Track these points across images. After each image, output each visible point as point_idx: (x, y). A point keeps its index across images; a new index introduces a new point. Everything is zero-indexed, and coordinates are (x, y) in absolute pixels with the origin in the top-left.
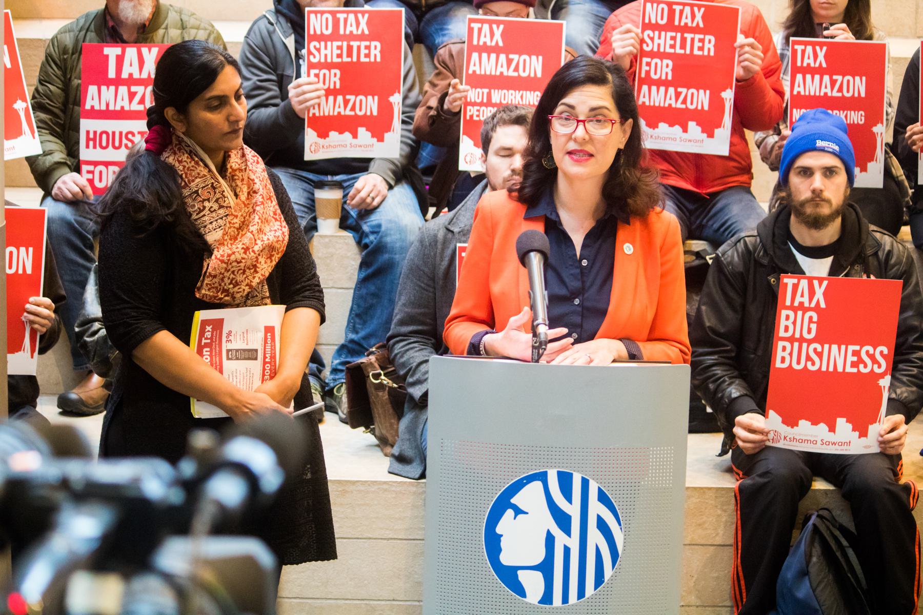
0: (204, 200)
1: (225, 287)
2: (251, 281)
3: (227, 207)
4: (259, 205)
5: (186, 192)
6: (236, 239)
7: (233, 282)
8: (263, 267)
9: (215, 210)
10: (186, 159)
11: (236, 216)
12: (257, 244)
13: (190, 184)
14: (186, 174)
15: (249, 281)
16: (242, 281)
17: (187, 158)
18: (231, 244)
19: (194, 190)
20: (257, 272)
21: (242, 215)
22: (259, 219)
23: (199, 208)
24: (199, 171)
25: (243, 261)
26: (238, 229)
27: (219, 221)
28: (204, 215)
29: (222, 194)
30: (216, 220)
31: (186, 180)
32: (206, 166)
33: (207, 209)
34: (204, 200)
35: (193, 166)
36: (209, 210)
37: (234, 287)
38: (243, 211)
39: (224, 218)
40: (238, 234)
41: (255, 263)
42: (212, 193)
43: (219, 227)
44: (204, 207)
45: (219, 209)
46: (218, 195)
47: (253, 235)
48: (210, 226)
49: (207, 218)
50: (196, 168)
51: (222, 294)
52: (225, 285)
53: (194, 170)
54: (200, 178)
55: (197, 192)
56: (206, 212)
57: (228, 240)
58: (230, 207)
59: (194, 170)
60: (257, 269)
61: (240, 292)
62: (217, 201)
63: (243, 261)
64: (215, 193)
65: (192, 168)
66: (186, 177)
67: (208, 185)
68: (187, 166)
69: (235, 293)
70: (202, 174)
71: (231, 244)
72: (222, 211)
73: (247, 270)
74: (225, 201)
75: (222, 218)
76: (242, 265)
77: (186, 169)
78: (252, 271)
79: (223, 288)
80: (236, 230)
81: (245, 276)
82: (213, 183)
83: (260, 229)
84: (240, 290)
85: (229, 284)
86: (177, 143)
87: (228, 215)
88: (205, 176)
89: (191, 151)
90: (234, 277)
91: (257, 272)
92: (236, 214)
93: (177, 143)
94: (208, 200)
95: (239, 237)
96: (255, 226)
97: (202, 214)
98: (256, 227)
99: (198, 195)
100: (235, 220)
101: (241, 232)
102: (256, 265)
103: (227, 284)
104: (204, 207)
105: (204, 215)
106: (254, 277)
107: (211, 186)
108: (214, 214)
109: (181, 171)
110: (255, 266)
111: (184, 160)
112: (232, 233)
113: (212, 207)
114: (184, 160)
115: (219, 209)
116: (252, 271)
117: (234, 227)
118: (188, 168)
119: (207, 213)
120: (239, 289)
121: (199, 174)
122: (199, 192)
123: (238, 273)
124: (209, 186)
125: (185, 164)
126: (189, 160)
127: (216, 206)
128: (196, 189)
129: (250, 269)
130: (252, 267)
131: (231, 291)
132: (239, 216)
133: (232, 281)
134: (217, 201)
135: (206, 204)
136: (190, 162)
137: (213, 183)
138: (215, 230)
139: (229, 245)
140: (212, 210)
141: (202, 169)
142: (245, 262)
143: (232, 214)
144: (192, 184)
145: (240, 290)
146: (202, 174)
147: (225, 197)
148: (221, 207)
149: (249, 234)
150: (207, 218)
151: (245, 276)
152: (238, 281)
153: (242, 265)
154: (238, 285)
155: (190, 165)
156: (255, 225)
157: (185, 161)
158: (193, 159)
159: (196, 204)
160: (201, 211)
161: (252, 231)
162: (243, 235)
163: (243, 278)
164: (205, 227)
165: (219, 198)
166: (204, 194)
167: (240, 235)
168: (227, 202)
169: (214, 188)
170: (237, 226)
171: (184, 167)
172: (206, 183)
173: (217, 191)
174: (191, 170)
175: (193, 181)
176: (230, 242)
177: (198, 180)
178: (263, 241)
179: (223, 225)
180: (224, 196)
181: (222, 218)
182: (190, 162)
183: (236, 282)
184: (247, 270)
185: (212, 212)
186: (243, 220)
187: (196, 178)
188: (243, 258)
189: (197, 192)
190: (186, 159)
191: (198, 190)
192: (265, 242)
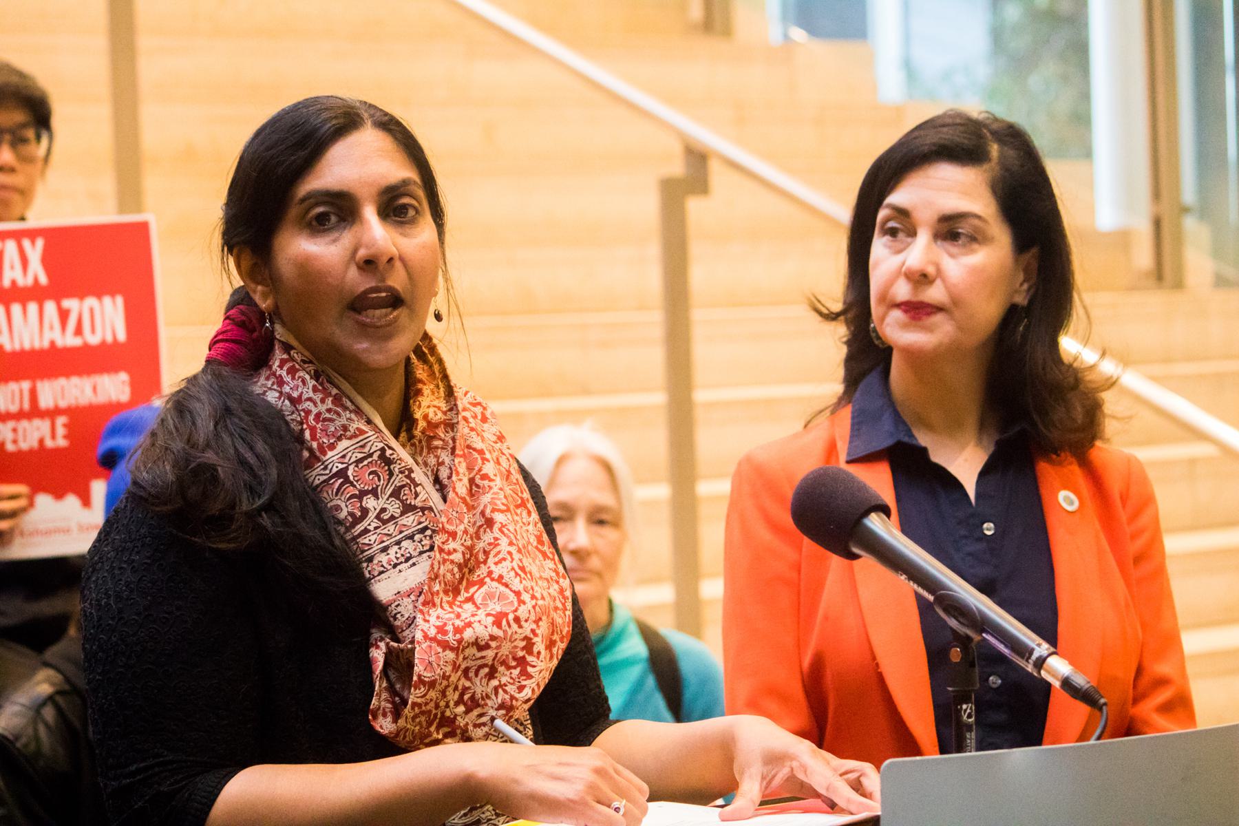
0: (363, 494)
1: (448, 713)
2: (512, 698)
3: (423, 509)
5: (317, 476)
6: (456, 592)
7: (466, 697)
9: (392, 518)
10: (311, 394)
11: (453, 535)
13: (325, 454)
14: (313, 430)
15: (507, 697)
16: (488, 697)
17: (315, 390)
18: (451, 604)
19: (335, 470)
20: (530, 677)
21: (466, 532)
23: (351, 514)
24: (346, 423)
26: (460, 566)
27: (404, 544)
28: (366, 531)
29: (408, 477)
30: (398, 543)
31: (315, 445)
33: (372, 515)
34: (363, 494)
35: (329, 411)
36: (378, 517)
37: (467, 712)
38: (466, 521)
39: (417, 537)
40: (461, 579)
41: (521, 654)
42: (384, 476)
43: (407, 560)
44: (365, 512)
45: (403, 514)
46: (399, 480)
47: (506, 585)
48: (383, 558)
49: (373, 538)
50: (339, 414)
51: (438, 733)
52: (447, 706)
54: (350, 438)
55: (342, 473)
56: (370, 522)
57: (441, 594)
58: (431, 509)
60: (530, 669)
61: (484, 724)
62: (396, 494)
64: (391, 474)
65: (328, 415)
66: (314, 437)
67: (371, 455)
68: (315, 411)
69: (470, 728)
71: (451, 604)
72: (410, 520)
74: (417, 495)
75: (411, 537)
77: (311, 418)
78: (516, 672)
79: (443, 713)
80: (456, 570)
81: (495, 683)
83: (522, 568)
84: (484, 719)
85: (457, 704)
86: (285, 356)
87: (426, 528)
88: (362, 432)
90: (468, 684)
91: (530, 677)
92: (450, 528)
93: (285, 356)
94: (374, 493)
95: (462, 587)
96: (504, 564)
97: (360, 528)
98: (507, 564)
99: (347, 480)
100: (451, 545)
102: (524, 657)
103: (452, 704)
104: (365, 512)
105: (366, 531)
106: (521, 688)
107: (380, 457)
108: (390, 528)
110: (522, 662)
111: (305, 396)
112: (449, 576)
113: (383, 510)
114: (305, 396)
115: (403, 514)
116: (516, 672)
117: (452, 562)
118: (318, 415)
119: (374, 525)
120: (481, 715)
121: (345, 428)
122: (350, 473)
123: (476, 675)
124: (375, 457)
125: (308, 405)
126: (318, 397)
127: (394, 508)
128: (341, 466)
129: (509, 668)
131: (461, 722)
132: (460, 533)
133: (462, 695)
134: (396, 494)
135: (370, 502)
136: (323, 401)
137: (383, 450)
138: (395, 566)
139: (446, 606)
140: (386, 516)
141: (353, 416)
143: (444, 530)
144: (330, 454)
145: (484, 719)
146: (353, 427)
147: (416, 485)
148: (408, 509)
149: (495, 584)
150: (373, 538)
152: (478, 696)
154: (478, 705)
155: (322, 408)
156: (504, 559)
157: (309, 399)
158: (327, 394)
159: (343, 505)
160: (357, 521)
161: (501, 577)
163: (489, 690)
164: (370, 559)
165: (403, 486)
166: (362, 478)
168: (422, 496)
169: (388, 462)
170: (458, 557)
172: (366, 450)
173: (396, 468)
174: (325, 420)
175: (332, 447)
176: (445, 599)
177: (344, 444)
178: (533, 597)
179: (414, 554)
180: (413, 480)
181: (411, 537)
182: (323, 401)
183: (473, 698)
184: (502, 669)
185: (385, 522)
186: (469, 543)
187: (339, 439)
189: (342, 473)
190: (311, 394)
191: (347, 468)
192: (540, 602)
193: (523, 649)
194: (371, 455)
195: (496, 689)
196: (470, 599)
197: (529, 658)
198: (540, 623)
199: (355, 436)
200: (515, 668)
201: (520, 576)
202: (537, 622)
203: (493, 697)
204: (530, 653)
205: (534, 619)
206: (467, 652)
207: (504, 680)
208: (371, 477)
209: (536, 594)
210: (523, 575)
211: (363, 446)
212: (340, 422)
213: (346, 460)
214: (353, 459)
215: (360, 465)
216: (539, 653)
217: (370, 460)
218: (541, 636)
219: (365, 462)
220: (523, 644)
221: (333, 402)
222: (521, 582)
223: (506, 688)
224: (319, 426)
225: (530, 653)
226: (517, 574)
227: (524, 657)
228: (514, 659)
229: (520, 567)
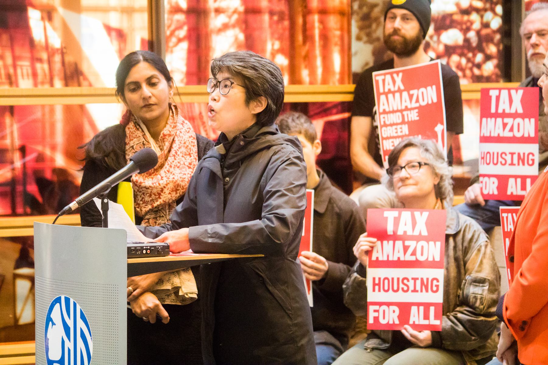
4: (170, 156)
8: (166, 196)
12: (163, 180)
20: (160, 198)
22: (168, 164)
25: (150, 188)
32: (143, 131)
40: (153, 173)
41: (159, 192)
50: (135, 132)
53: (134, 133)
55: (132, 147)
59: (134, 133)
63: (150, 188)
65: (134, 132)
67: (140, 143)
70: (138, 136)
73: (153, 196)
76: (149, 191)
78: (157, 197)
82: (143, 141)
88: (140, 136)
89: (136, 122)
91: (160, 198)
95: (153, 175)
99: (133, 148)
101: (156, 172)
102: (160, 193)
107: (143, 143)
109: (128, 134)
110: (159, 194)
116: (157, 197)
121: (136, 136)
122: (134, 147)
124: (142, 143)
128: (133, 145)
129: (155, 195)
130: (157, 194)
142: (151, 190)
146: (138, 136)
151: (151, 199)
153: (149, 191)
155: (133, 130)
159: (130, 154)
162: (156, 175)
167: (154, 174)
169: (144, 144)
171: (130, 131)
175: (132, 140)
177: (135, 139)
182: (133, 128)
187: (134, 138)
188: (150, 187)
189: (132, 147)
193: (160, 191)
194: (140, 143)
195: (151, 200)
196: (152, 178)
197: (162, 194)
198: (168, 185)
199: (138, 138)
200: (157, 195)
201: (166, 173)
202: (167, 185)
203: (150, 202)
204: (162, 192)
205: (166, 183)
206: (143, 189)
207: (153, 198)
208: (139, 148)
209: (170, 177)
210: (167, 172)
211: (139, 140)
212: (136, 134)
213: (135, 144)
214: (136, 143)
215: (137, 145)
216: (165, 192)
217: (140, 144)
218: (167, 189)
219: (139, 144)
220: (161, 190)
221: (135, 129)
222: (166, 174)
223: (154, 201)
224: (132, 135)
225: (162, 192)
226: (165, 172)
227: (160, 193)
228: (158, 193)
229: (167, 171)
